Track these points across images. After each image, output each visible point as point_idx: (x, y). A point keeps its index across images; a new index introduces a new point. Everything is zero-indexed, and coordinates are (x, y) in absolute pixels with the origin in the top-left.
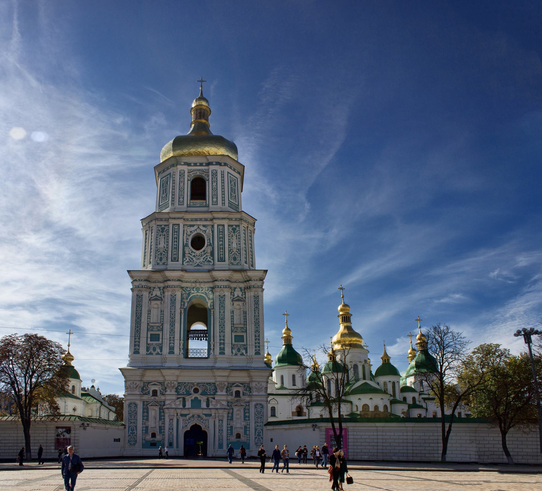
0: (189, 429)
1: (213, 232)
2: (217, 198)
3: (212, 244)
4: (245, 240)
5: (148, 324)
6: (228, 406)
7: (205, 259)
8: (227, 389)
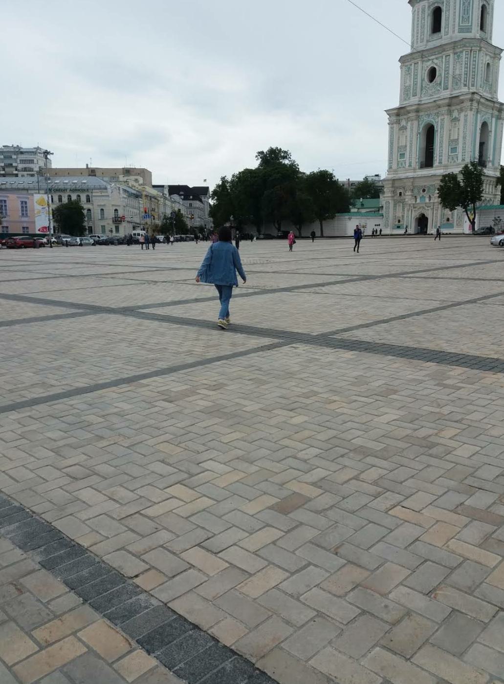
0: (418, 217)
2: (448, 28)
5: (398, 147)
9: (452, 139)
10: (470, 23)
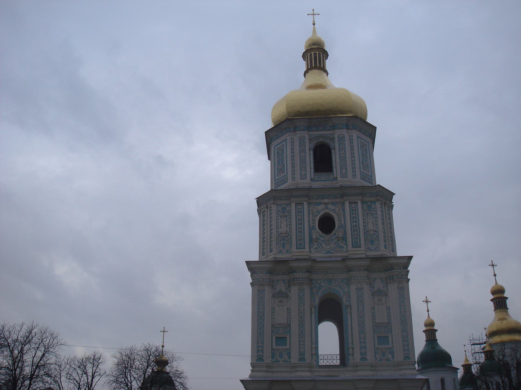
1: (344, 210)
2: (346, 169)
3: (344, 226)
4: (383, 219)
5: (272, 325)
7: (336, 244)
10: (370, 172)
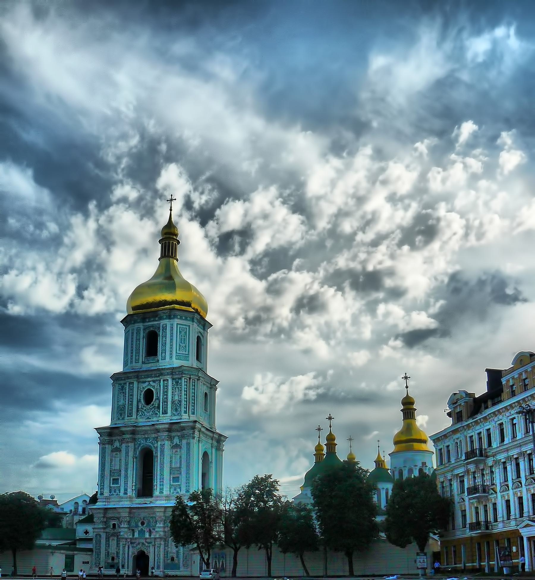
0: (136, 554)
1: (160, 385)
5: (110, 471)
6: (165, 535)
8: (164, 522)
9: (173, 467)
